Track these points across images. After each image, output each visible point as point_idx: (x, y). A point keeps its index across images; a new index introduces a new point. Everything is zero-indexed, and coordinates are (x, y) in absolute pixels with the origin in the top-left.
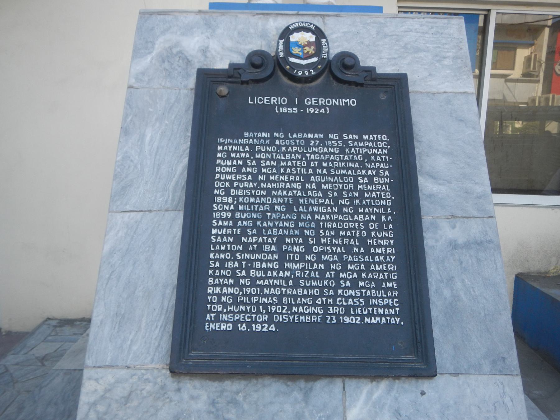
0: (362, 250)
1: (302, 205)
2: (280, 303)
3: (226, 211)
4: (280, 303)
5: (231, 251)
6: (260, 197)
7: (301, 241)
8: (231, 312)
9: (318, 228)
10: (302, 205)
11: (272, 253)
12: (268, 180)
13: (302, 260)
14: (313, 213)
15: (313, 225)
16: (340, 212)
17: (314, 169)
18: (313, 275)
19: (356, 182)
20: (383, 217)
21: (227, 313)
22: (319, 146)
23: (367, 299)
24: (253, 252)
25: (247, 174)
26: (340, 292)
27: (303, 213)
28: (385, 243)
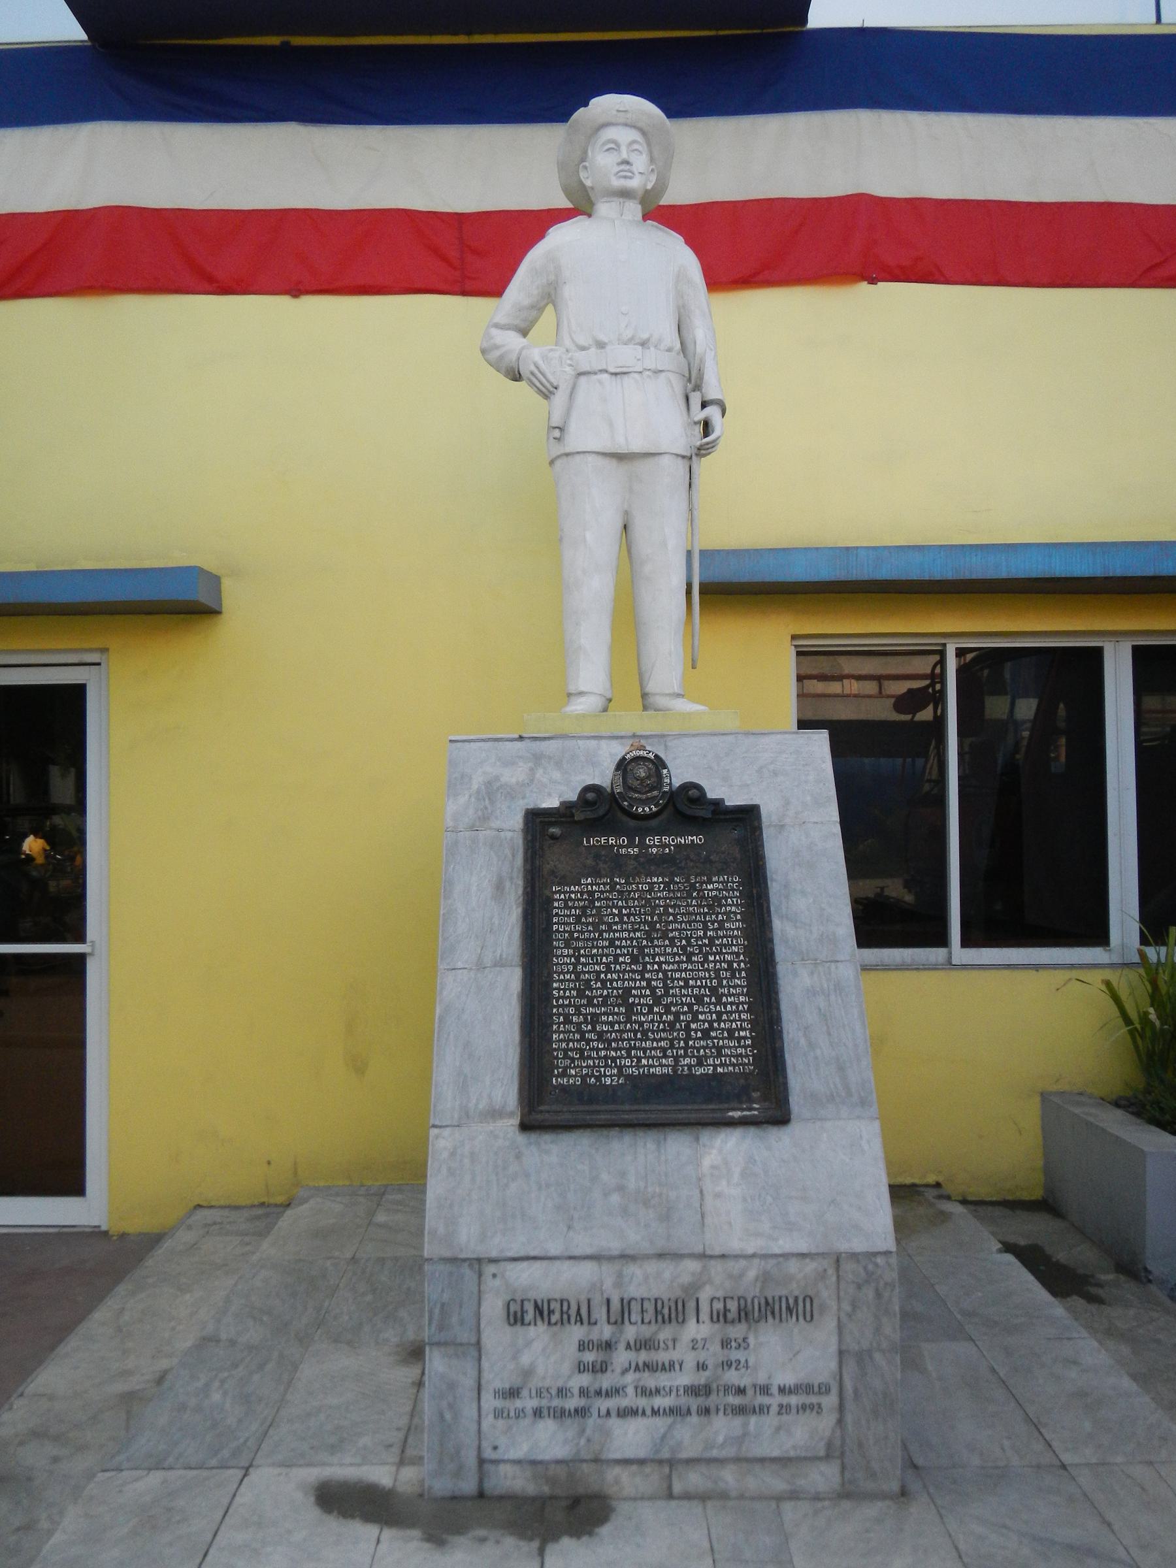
0: (713, 999)
2: (629, 1056)
3: (567, 964)
5: (574, 1006)
6: (602, 948)
7: (648, 992)
8: (578, 1066)
9: (664, 980)
11: (619, 1006)
12: (610, 930)
13: (651, 1011)
14: (660, 964)
16: (689, 961)
17: (660, 915)
18: (661, 1026)
19: (706, 929)
20: (735, 965)
21: (575, 1067)
23: (719, 1049)
24: (598, 1006)
25: (588, 924)
27: (650, 963)
28: (737, 992)
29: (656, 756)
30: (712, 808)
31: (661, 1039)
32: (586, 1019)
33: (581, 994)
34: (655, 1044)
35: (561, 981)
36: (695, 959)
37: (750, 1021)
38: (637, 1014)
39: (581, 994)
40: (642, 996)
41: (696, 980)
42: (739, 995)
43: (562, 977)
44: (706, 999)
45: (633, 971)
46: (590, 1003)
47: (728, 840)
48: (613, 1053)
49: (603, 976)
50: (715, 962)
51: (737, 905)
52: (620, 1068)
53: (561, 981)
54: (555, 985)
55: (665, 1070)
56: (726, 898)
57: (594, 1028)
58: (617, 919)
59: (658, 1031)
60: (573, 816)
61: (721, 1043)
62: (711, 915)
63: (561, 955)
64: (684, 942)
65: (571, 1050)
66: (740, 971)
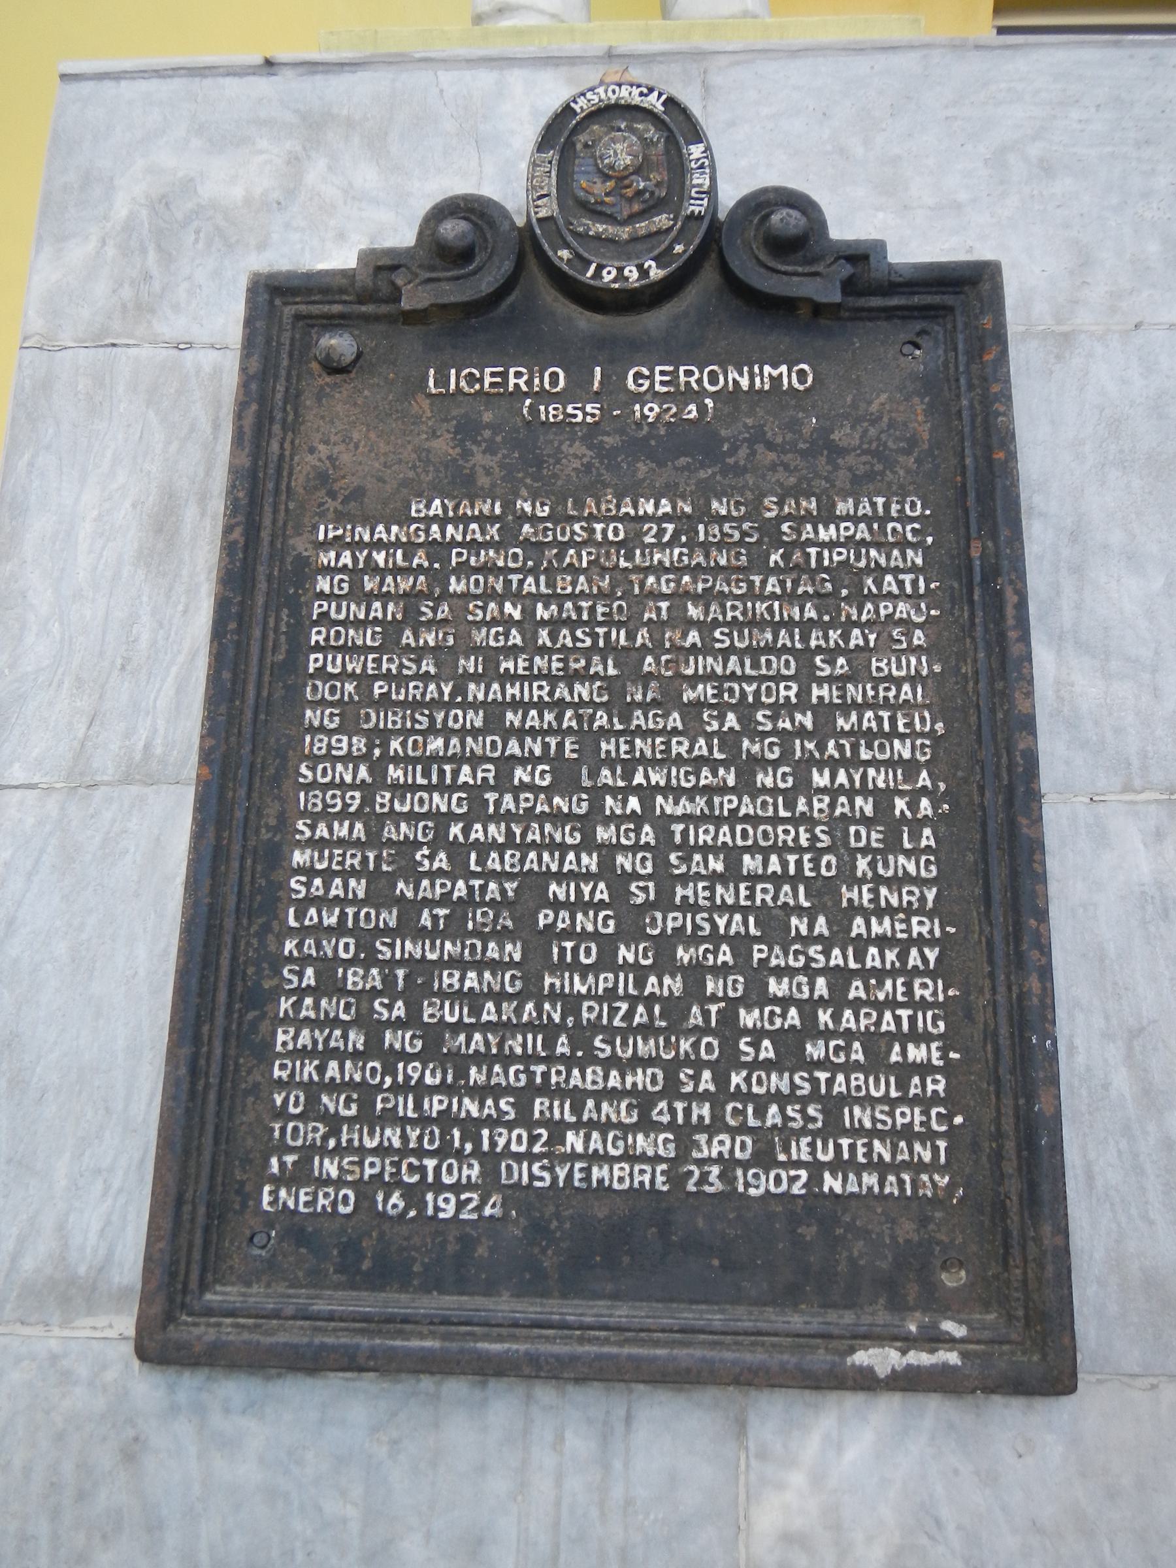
1: (611, 762)
2: (524, 1118)
4: (524, 1118)
9: (659, 851)
10: (611, 762)
11: (502, 936)
13: (607, 961)
14: (647, 793)
15: (648, 834)
16: (747, 786)
20: (900, 804)
22: (674, 541)
23: (833, 1106)
26: (736, 1079)
27: (613, 791)
29: (671, 102)
30: (846, 270)
31: (637, 1062)
32: (389, 980)
33: (379, 896)
34: (614, 1081)
35: (318, 844)
36: (765, 779)
37: (946, 1009)
38: (560, 967)
39: (379, 896)
40: (580, 905)
41: (766, 853)
42: (909, 911)
43: (322, 831)
44: (799, 924)
45: (558, 818)
46: (408, 928)
47: (888, 378)
48: (471, 1107)
49: (455, 830)
50: (833, 792)
51: (914, 597)
52: (491, 1160)
53: (318, 844)
54: (299, 858)
55: (643, 1176)
56: (879, 572)
57: (414, 1011)
58: (516, 638)
59: (630, 1031)
60: (395, 296)
61: (840, 1086)
62: (825, 628)
63: (328, 757)
64: (731, 720)
65: (333, 1087)
66: (916, 825)
